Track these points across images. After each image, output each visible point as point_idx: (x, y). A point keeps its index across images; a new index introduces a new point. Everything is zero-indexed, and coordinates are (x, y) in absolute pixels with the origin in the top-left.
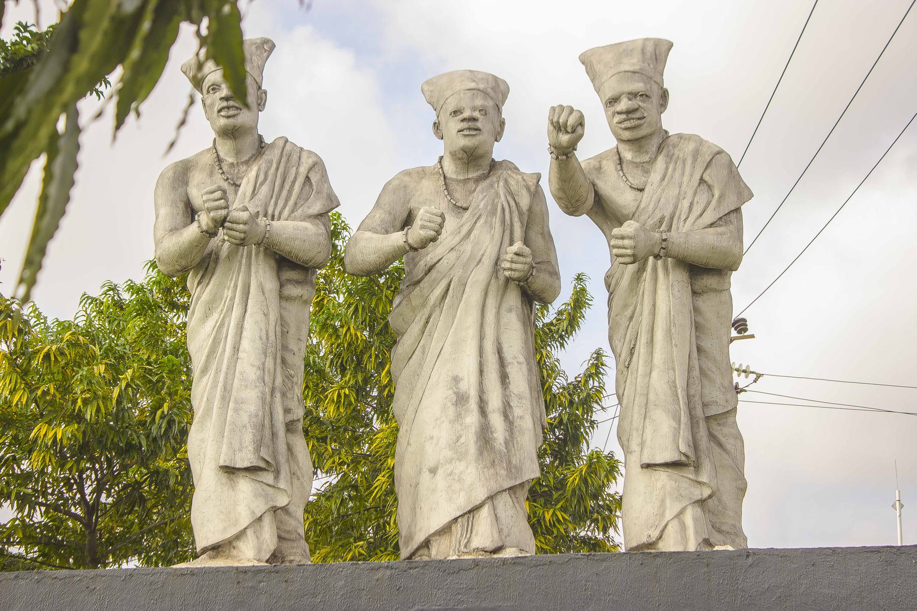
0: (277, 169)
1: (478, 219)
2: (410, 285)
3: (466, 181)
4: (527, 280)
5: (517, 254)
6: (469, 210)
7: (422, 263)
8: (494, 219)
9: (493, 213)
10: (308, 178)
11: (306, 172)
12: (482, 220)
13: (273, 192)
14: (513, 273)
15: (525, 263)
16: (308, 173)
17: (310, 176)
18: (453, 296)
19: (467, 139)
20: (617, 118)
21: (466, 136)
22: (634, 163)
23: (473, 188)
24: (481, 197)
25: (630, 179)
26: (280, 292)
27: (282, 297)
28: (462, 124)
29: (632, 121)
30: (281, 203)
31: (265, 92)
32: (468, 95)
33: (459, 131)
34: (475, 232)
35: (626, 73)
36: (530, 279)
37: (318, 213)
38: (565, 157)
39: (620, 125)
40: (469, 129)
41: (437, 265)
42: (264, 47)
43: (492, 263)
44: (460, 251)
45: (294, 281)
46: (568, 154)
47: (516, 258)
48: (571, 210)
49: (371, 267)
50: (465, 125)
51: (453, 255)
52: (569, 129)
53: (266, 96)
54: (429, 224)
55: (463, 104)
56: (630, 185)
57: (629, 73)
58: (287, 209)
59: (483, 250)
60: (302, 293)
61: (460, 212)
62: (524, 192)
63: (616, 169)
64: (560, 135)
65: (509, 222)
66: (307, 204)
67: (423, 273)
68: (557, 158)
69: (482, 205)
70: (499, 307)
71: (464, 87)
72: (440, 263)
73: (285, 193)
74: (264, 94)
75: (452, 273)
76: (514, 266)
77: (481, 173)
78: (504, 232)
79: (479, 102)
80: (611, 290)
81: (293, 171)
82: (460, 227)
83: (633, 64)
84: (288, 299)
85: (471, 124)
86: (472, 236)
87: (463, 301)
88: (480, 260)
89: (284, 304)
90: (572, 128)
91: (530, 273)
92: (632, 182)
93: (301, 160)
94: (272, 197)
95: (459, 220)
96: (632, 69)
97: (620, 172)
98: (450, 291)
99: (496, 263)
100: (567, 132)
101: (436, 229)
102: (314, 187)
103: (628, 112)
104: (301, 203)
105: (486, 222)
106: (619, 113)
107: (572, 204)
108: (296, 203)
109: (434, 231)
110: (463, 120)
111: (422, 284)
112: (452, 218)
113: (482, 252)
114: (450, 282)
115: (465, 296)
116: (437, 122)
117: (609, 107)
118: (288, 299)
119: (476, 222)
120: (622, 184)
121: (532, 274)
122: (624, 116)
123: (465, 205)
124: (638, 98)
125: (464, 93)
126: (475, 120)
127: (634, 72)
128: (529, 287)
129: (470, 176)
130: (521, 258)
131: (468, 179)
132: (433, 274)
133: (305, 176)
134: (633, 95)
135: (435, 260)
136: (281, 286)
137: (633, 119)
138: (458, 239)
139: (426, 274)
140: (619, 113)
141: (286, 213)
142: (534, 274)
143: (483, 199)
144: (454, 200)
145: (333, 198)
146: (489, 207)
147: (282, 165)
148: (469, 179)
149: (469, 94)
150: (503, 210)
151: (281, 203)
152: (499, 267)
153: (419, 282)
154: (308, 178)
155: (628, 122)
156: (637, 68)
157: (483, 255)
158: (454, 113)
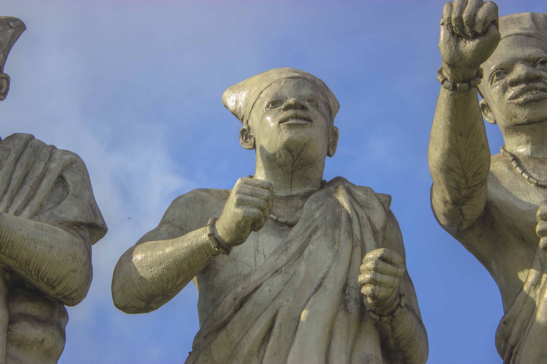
0: (17, 160)
1: (314, 232)
2: (210, 333)
3: (289, 198)
4: (392, 314)
5: (382, 259)
6: (296, 229)
7: (229, 298)
8: (337, 232)
9: (336, 224)
10: (61, 179)
11: (59, 169)
12: (319, 233)
13: (8, 185)
14: (378, 288)
15: (395, 275)
16: (63, 170)
17: (65, 175)
18: (280, 337)
19: (293, 131)
20: (511, 92)
21: (290, 126)
22: (534, 158)
23: (300, 205)
24: (314, 206)
25: (535, 175)
26: (8, 330)
27: (10, 340)
28: (285, 113)
29: (534, 92)
30: (19, 201)
31: (7, 79)
32: (292, 83)
33: (281, 122)
34: (311, 247)
35: (519, 37)
36: (398, 311)
37: (75, 220)
38: (466, 85)
39: (515, 101)
40: (296, 117)
41: (255, 296)
42: (9, 24)
43: (338, 288)
44: (288, 273)
45: (32, 317)
46: (470, 80)
47: (382, 264)
48: (464, 192)
49: (154, 288)
50: (291, 112)
51: (278, 280)
52: (479, 30)
53: (8, 84)
54: (250, 198)
55: (286, 93)
56: (535, 182)
57: (523, 37)
58: (28, 208)
59: (324, 271)
60: (44, 336)
61: (283, 230)
62: (376, 204)
63: (510, 168)
64: (462, 43)
65: (359, 237)
66: (59, 207)
67: (232, 310)
68: (454, 88)
69: (317, 215)
70: (351, 355)
71: (284, 76)
72: (258, 292)
73: (26, 189)
74: (5, 81)
75: (279, 301)
76: (379, 277)
77: (310, 189)
78: (353, 248)
79: (306, 92)
80: (512, 341)
81: (40, 167)
82: (286, 244)
83: (526, 29)
84: (21, 344)
85: (300, 113)
86: (306, 252)
87: (297, 341)
88: (320, 286)
89: (13, 351)
90: (484, 24)
91: (396, 303)
92: (538, 178)
93: (54, 156)
94: (5, 192)
95: (282, 239)
96: (525, 32)
97: (519, 170)
98: (276, 330)
99: (344, 291)
100: (475, 36)
101: (263, 204)
102: (71, 188)
103: (528, 79)
104: (50, 206)
105: (325, 235)
106: (514, 83)
107: (467, 181)
108: (42, 206)
109: (259, 208)
110: (287, 108)
111: (229, 327)
112: (272, 237)
113: (321, 275)
114: (275, 315)
115: (299, 333)
116: (245, 127)
117: (497, 80)
118: (21, 344)
119: (310, 236)
120: (521, 184)
121: (399, 305)
122: (523, 86)
123: (290, 220)
124: (539, 67)
125: (286, 82)
126: (303, 108)
127: (528, 36)
128: (393, 329)
129: (294, 192)
130: (390, 266)
131: (292, 196)
132: (248, 308)
133: (57, 172)
134: (530, 62)
135: (250, 289)
136: (12, 321)
137: (536, 89)
138: (284, 258)
139: (236, 311)
140: (514, 83)
141: (26, 213)
142: (403, 304)
143: (319, 208)
144: (274, 215)
145: (97, 213)
146: (329, 217)
147: (24, 159)
148: (294, 196)
149: (293, 82)
150: (350, 219)
151: (19, 201)
152: (348, 297)
153: (224, 325)
154: (61, 179)
155: (529, 93)
156: (532, 32)
157: (323, 279)
158: (273, 105)
